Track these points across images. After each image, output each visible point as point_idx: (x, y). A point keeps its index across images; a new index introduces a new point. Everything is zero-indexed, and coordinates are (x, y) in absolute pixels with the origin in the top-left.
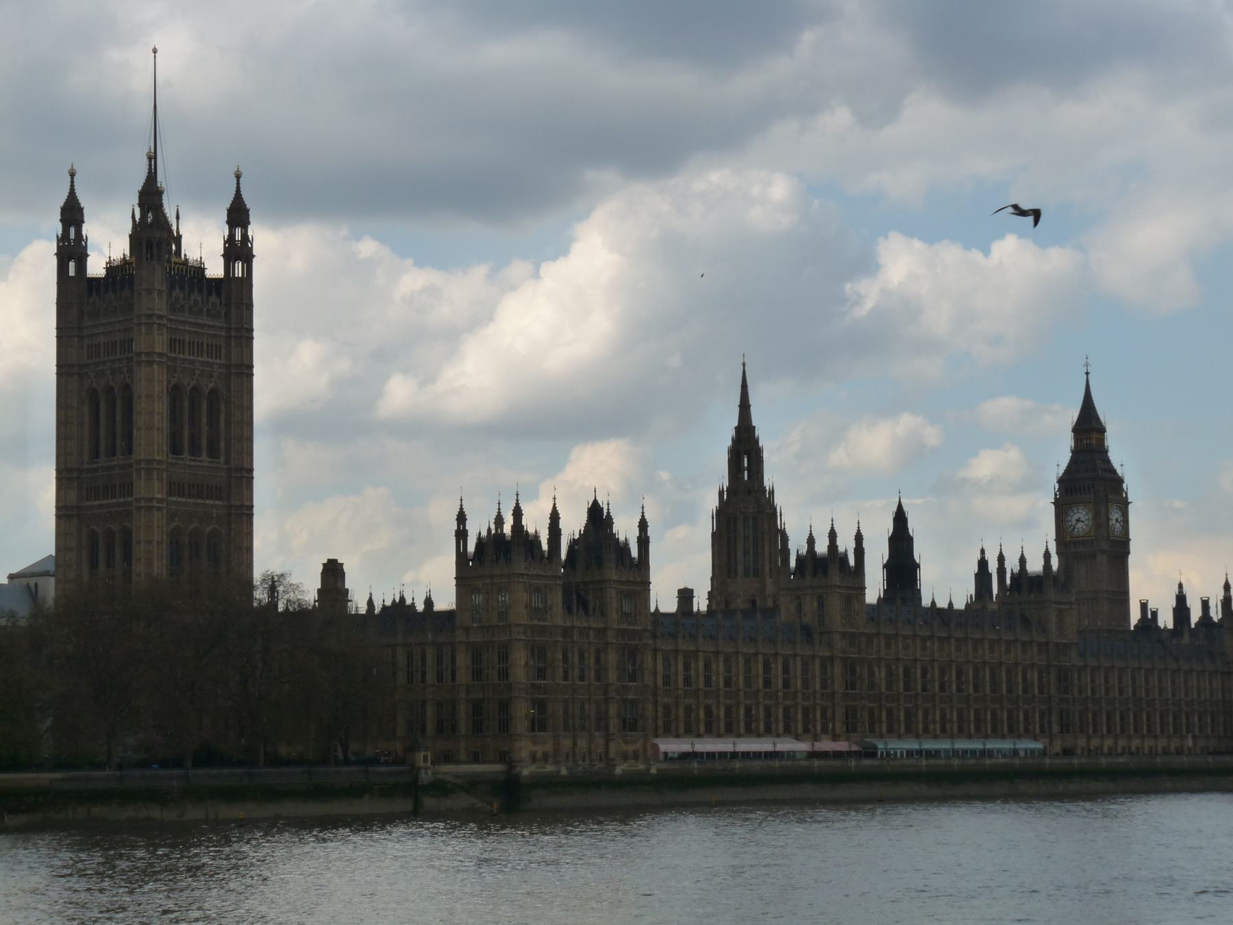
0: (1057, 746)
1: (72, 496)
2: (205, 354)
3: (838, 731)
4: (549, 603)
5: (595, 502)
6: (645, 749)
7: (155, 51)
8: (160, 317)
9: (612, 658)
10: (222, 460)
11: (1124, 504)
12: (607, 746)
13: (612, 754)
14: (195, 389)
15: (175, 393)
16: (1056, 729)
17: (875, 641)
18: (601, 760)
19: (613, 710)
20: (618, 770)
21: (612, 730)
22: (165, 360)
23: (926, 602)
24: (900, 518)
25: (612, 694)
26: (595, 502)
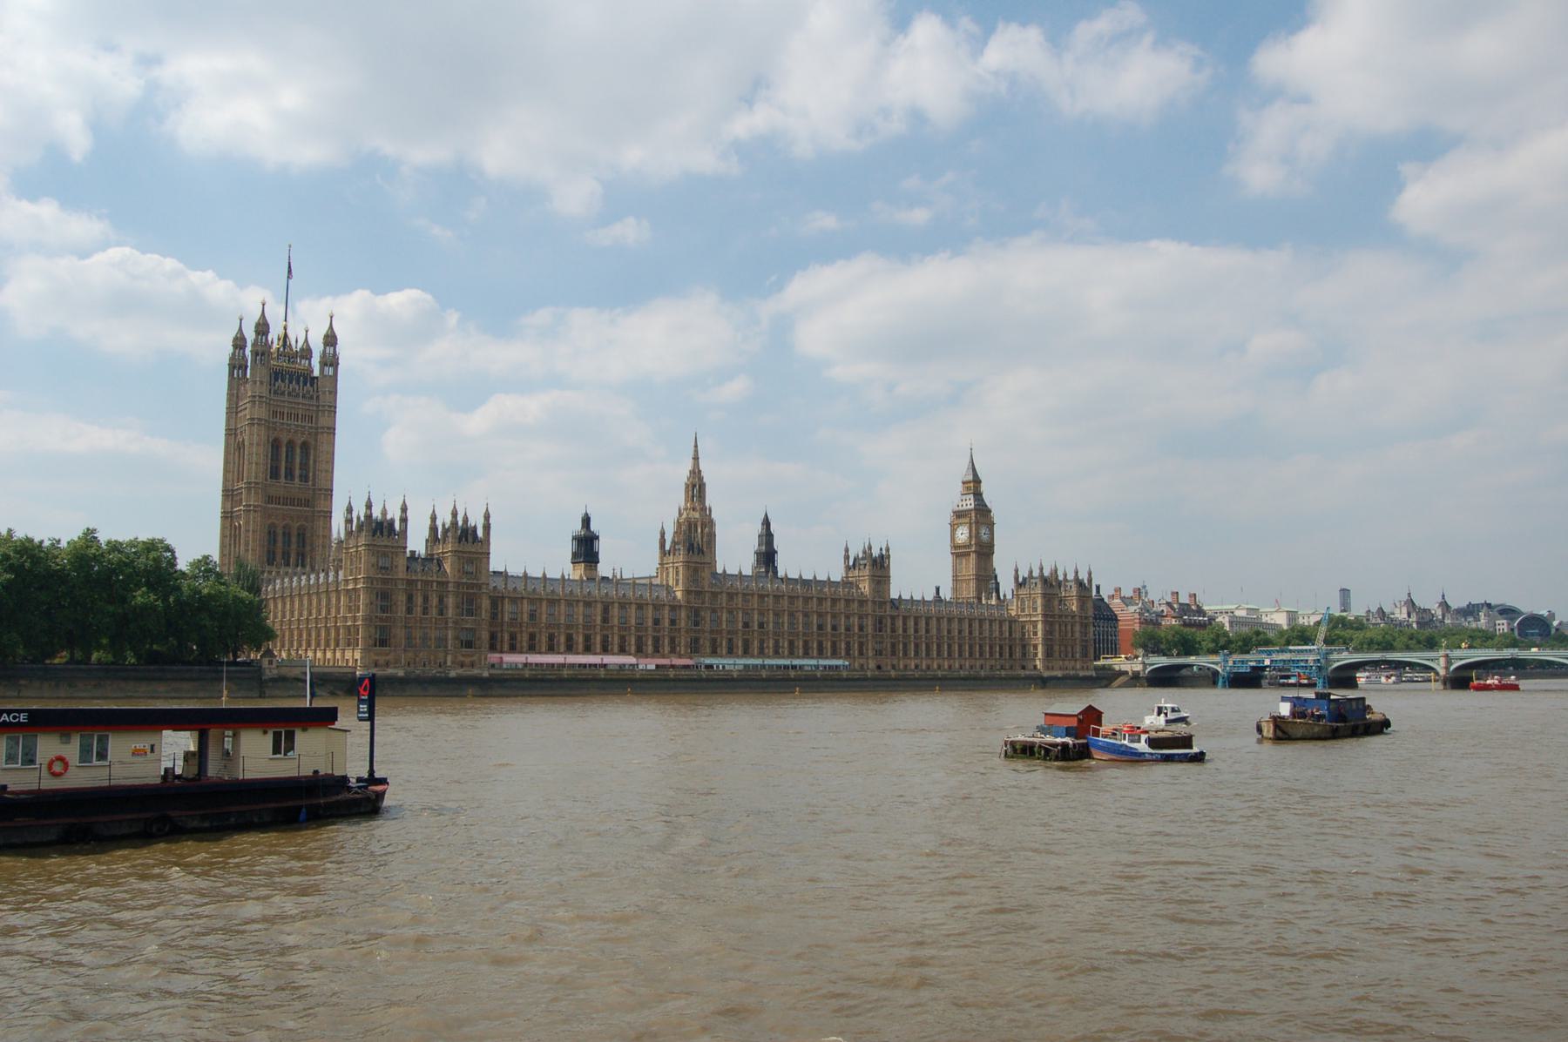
0: (872, 664)
1: (229, 505)
2: (300, 421)
3: (682, 652)
4: (394, 563)
5: (586, 514)
6: (480, 660)
7: (290, 246)
8: (260, 397)
9: (451, 601)
10: (310, 483)
11: (991, 525)
12: (446, 657)
13: (449, 663)
14: (291, 444)
15: (275, 445)
16: (870, 653)
17: (719, 596)
18: (440, 666)
19: (450, 634)
20: (453, 674)
21: (449, 648)
22: (263, 422)
23: (781, 574)
24: (766, 523)
25: (450, 625)
26: (586, 514)
